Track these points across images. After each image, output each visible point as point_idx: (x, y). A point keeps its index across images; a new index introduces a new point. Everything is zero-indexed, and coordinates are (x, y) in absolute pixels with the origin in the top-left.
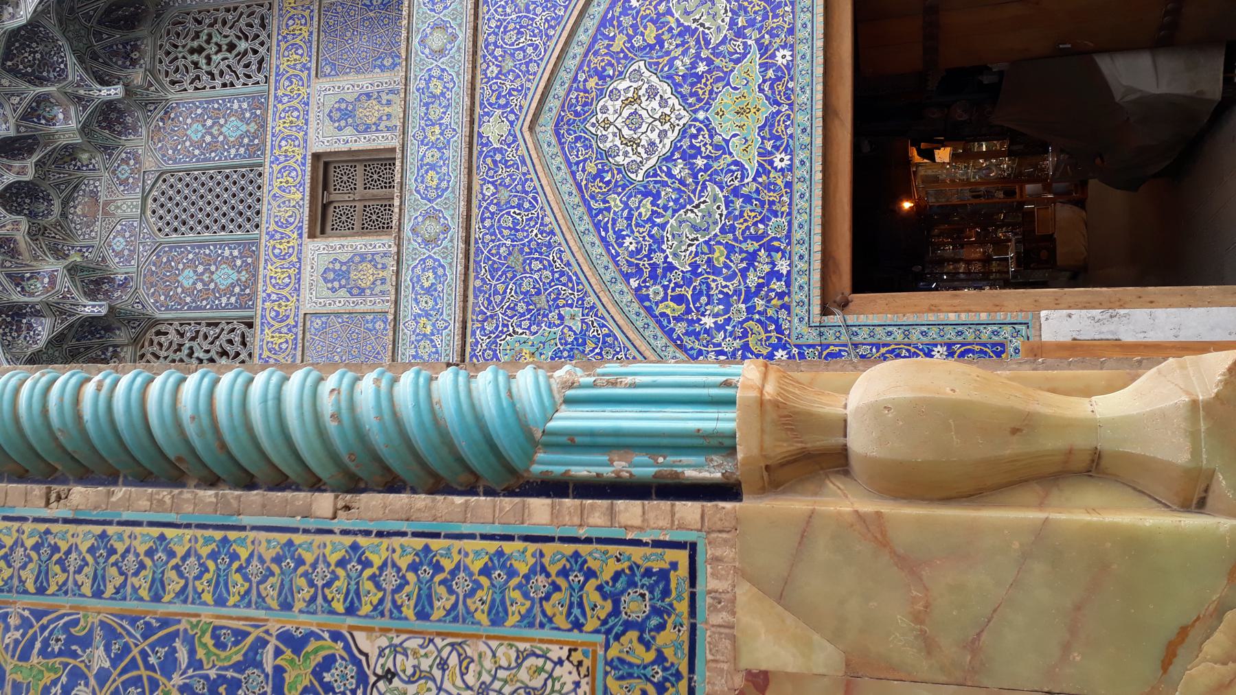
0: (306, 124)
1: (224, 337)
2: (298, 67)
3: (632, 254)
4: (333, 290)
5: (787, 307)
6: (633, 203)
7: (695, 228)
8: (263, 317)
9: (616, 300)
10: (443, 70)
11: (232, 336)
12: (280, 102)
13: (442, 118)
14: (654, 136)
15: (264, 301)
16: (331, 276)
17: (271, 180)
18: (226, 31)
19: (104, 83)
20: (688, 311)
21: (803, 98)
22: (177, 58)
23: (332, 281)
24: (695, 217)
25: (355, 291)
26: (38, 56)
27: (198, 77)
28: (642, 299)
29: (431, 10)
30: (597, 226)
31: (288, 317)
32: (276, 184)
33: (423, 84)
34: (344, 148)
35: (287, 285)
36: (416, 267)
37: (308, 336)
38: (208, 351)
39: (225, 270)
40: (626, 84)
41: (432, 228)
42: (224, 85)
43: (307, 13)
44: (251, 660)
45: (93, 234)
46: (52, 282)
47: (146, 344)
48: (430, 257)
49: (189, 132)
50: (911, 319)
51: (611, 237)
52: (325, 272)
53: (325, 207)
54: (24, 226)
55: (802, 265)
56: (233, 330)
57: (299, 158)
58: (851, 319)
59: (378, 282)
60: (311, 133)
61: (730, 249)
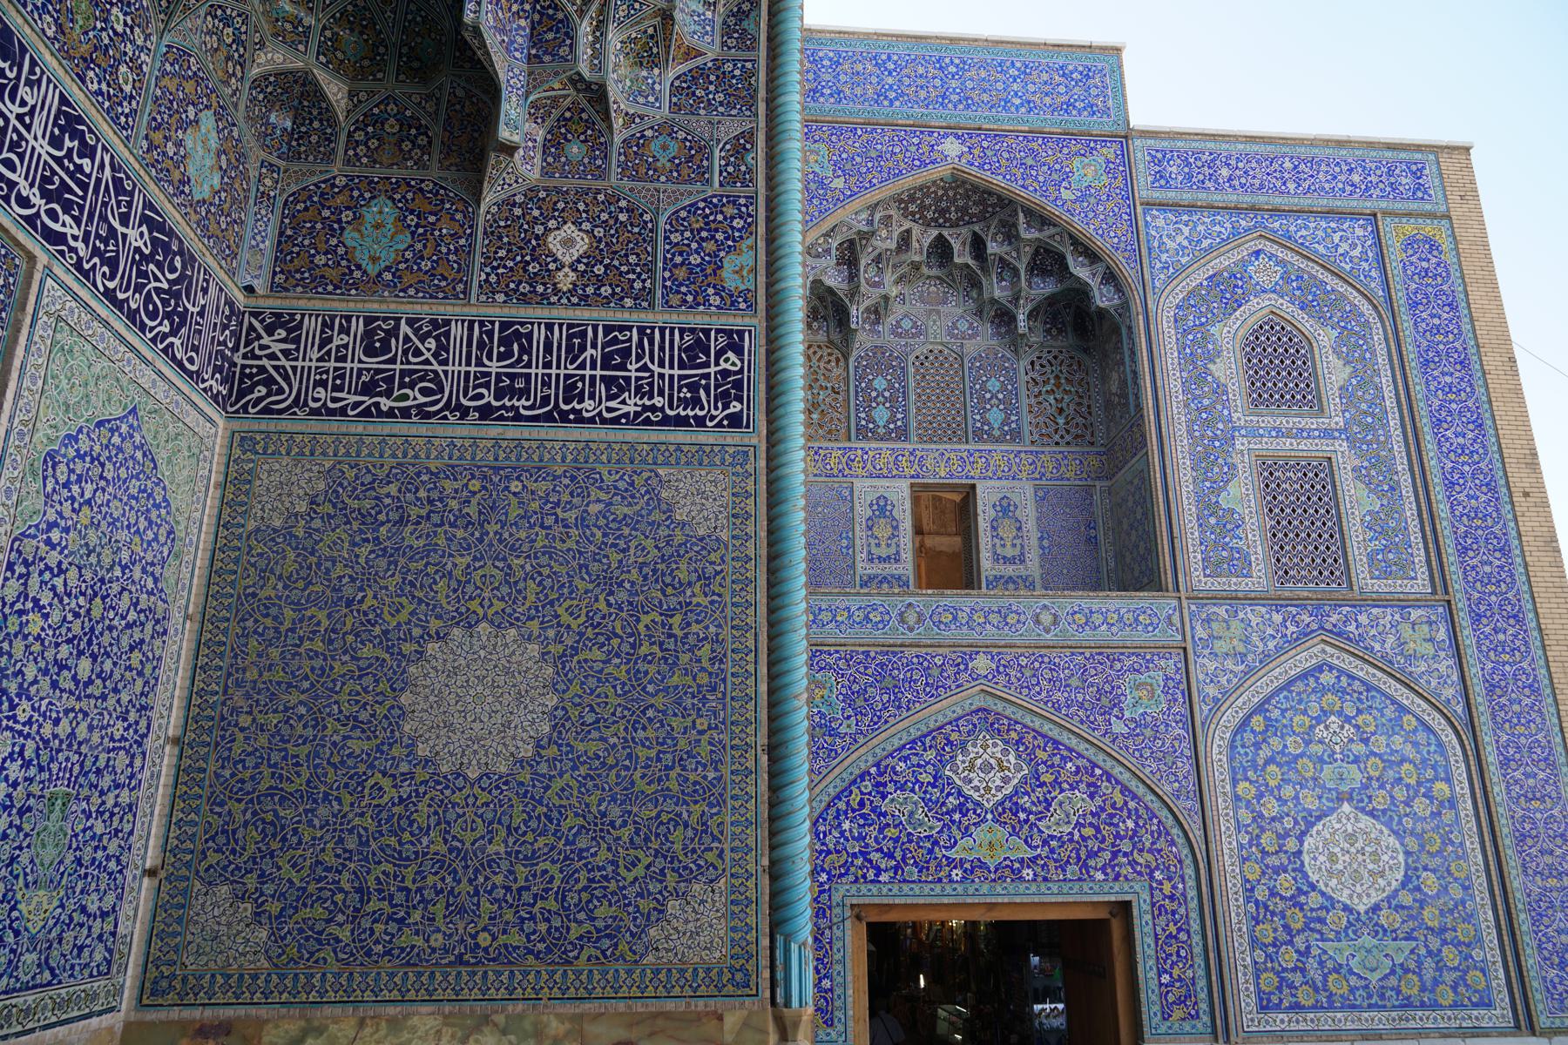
3: (893, 768)
4: (871, 505)
5: (857, 880)
6: (930, 768)
7: (911, 814)
9: (862, 758)
14: (976, 782)
19: (1030, 316)
20: (854, 811)
21: (999, 889)
24: (919, 815)
28: (862, 777)
30: (914, 742)
32: (952, 455)
34: (979, 511)
39: (886, 415)
40: (1013, 761)
41: (911, 618)
44: (714, 838)
50: (849, 965)
51: (906, 752)
54: (917, 258)
55: (885, 891)
58: (848, 923)
61: (896, 840)
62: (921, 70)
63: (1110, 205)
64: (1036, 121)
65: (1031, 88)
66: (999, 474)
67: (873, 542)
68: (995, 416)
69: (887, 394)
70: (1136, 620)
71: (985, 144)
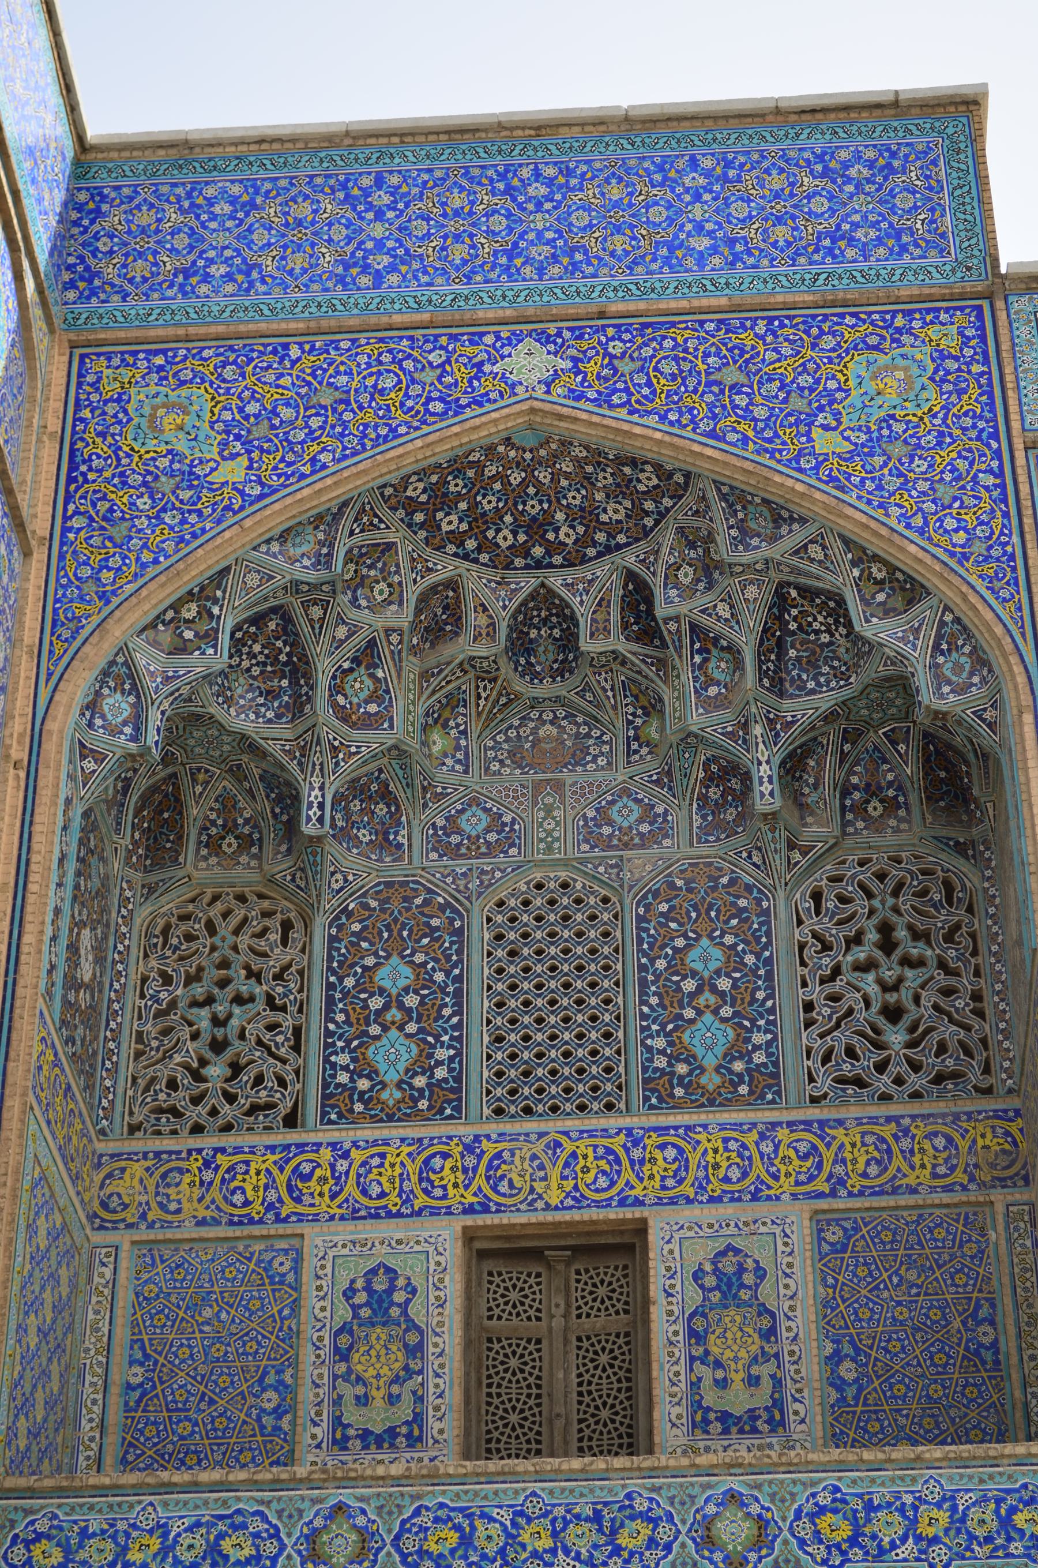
0: (712, 1200)
1: (270, 1067)
2: (839, 1170)
4: (349, 1293)
8: (301, 1147)
10: (668, 1547)
11: (271, 1083)
12: (762, 1136)
13: (567, 1552)
15: (333, 1145)
16: (380, 1284)
17: (591, 1133)
18: (929, 998)
22: (870, 895)
23: (368, 1289)
25: (344, 1340)
26: (825, 638)
27: (826, 947)
29: (798, 1515)
31: (298, 1200)
32: (583, 1146)
33: (641, 1505)
34: (655, 1290)
35: (364, 1192)
36: (265, 1519)
37: (258, 1247)
38: (242, 1036)
42: (809, 1007)
43: (960, 1176)
45: (495, 767)
46: (370, 722)
47: (266, 904)
48: (282, 1547)
49: (705, 942)
52: (388, 1270)
53: (536, 1254)
54: (481, 650)
56: (282, 1083)
57: (638, 1192)
59: (360, 1390)
60: (687, 1214)
62: (457, 200)
63: (946, 455)
64: (749, 284)
65: (739, 210)
66: (715, 1187)
67: (348, 1391)
68: (709, 1037)
69: (411, 1001)
70: (1006, 1522)
71: (616, 348)
